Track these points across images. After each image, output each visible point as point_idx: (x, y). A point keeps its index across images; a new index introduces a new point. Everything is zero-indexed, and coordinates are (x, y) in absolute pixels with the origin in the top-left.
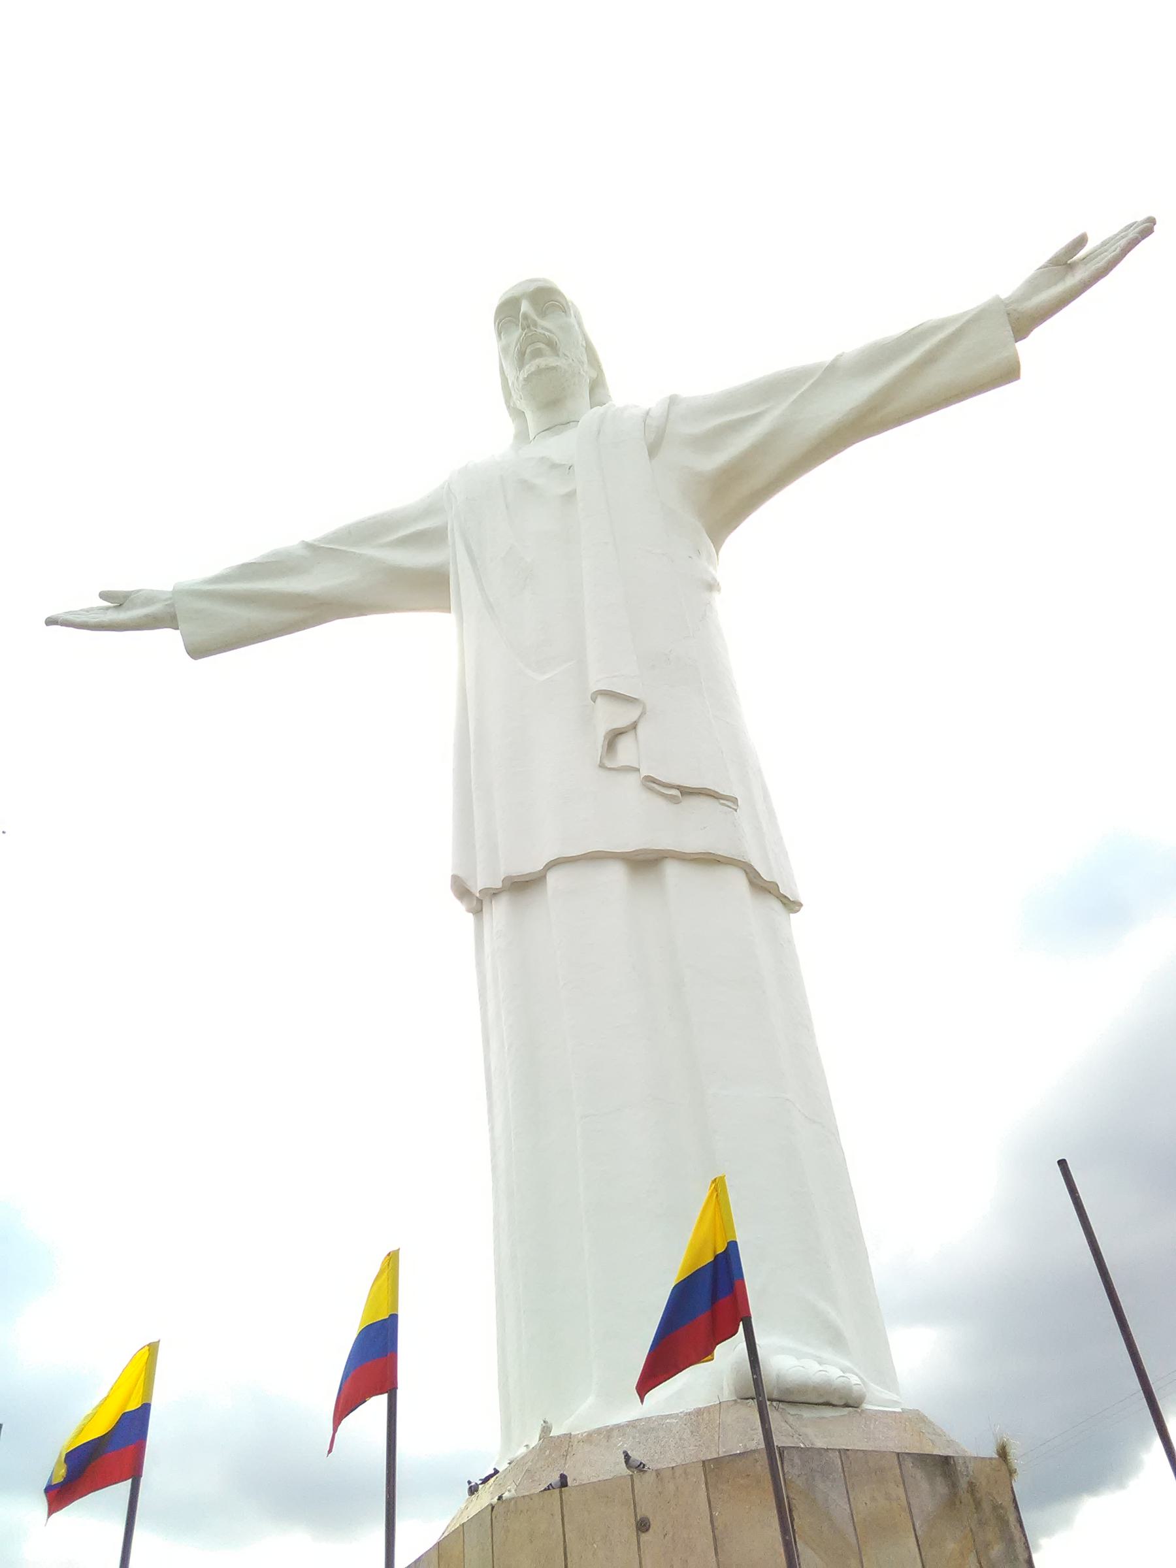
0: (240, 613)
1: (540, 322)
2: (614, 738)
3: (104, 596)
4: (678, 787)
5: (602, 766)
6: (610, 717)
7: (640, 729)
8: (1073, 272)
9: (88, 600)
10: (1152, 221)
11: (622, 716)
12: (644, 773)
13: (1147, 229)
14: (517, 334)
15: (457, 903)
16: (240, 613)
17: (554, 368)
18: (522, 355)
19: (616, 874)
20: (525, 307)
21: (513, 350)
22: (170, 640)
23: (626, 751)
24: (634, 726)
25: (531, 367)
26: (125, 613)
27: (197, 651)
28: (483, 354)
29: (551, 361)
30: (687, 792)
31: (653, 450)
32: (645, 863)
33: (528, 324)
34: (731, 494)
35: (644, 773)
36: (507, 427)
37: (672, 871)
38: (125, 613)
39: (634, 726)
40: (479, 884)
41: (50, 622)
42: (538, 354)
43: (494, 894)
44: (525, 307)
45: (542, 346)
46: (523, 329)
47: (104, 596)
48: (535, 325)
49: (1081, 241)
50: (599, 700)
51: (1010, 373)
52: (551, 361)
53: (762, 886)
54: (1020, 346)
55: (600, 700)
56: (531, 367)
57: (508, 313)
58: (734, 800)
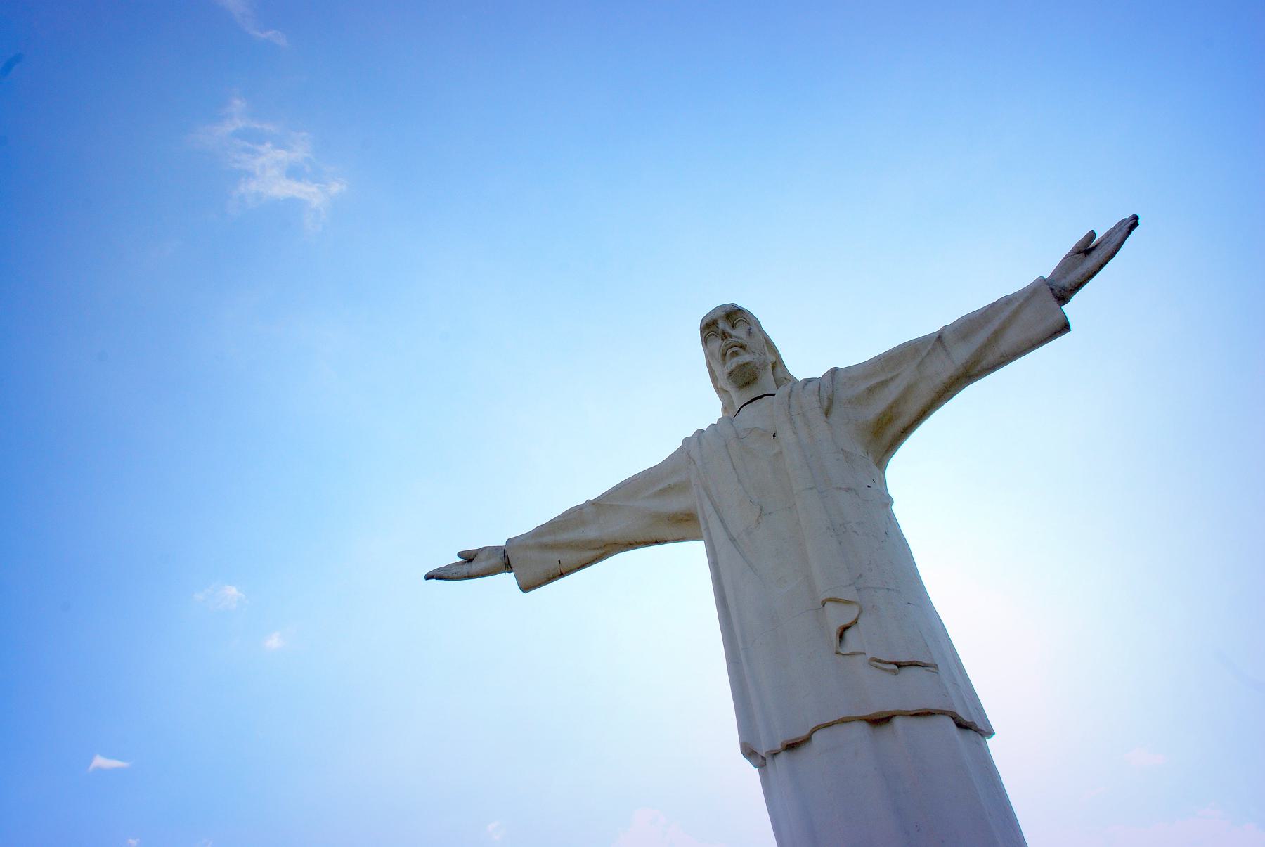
0: (550, 554)
1: (733, 333)
3: (460, 555)
4: (895, 663)
5: (837, 653)
6: (836, 617)
7: (860, 622)
8: (1091, 256)
9: (450, 558)
10: (1136, 218)
12: (869, 656)
13: (1134, 223)
14: (717, 344)
15: (747, 763)
16: (550, 554)
18: (724, 355)
19: (861, 729)
20: (722, 325)
21: (718, 354)
22: (507, 580)
24: (856, 622)
26: (472, 565)
27: (526, 588)
28: (692, 355)
29: (745, 358)
30: (900, 665)
31: (827, 414)
32: (880, 721)
33: (725, 335)
34: (889, 432)
36: (718, 404)
37: (898, 722)
38: (472, 565)
39: (856, 622)
40: (763, 750)
41: (429, 577)
42: (735, 354)
44: (722, 325)
47: (460, 555)
48: (730, 336)
49: (1092, 235)
50: (828, 604)
51: (1065, 328)
52: (745, 358)
53: (962, 725)
54: (1066, 308)
56: (732, 363)
57: (710, 328)
58: (936, 666)
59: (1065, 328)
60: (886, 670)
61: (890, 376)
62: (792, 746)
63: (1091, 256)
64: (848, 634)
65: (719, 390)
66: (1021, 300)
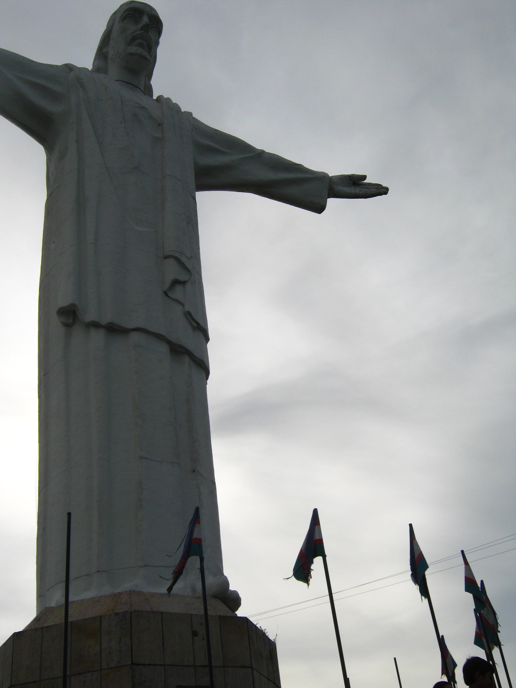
2: (176, 282)
4: (198, 323)
5: (166, 293)
6: (172, 271)
7: (188, 286)
8: (355, 187)
11: (183, 277)
17: (145, 58)
18: (134, 39)
19: (164, 349)
20: (145, 19)
23: (178, 293)
24: (184, 283)
25: (133, 49)
32: (178, 351)
35: (187, 308)
39: (184, 283)
42: (141, 45)
43: (95, 325)
45: (145, 43)
46: (141, 29)
49: (364, 177)
51: (319, 209)
52: (148, 57)
55: (171, 261)
56: (133, 49)
59: (319, 209)
60: (191, 324)
61: (224, 150)
62: (113, 330)
63: (355, 187)
64: (179, 288)
65: (102, 53)
66: (312, 176)
